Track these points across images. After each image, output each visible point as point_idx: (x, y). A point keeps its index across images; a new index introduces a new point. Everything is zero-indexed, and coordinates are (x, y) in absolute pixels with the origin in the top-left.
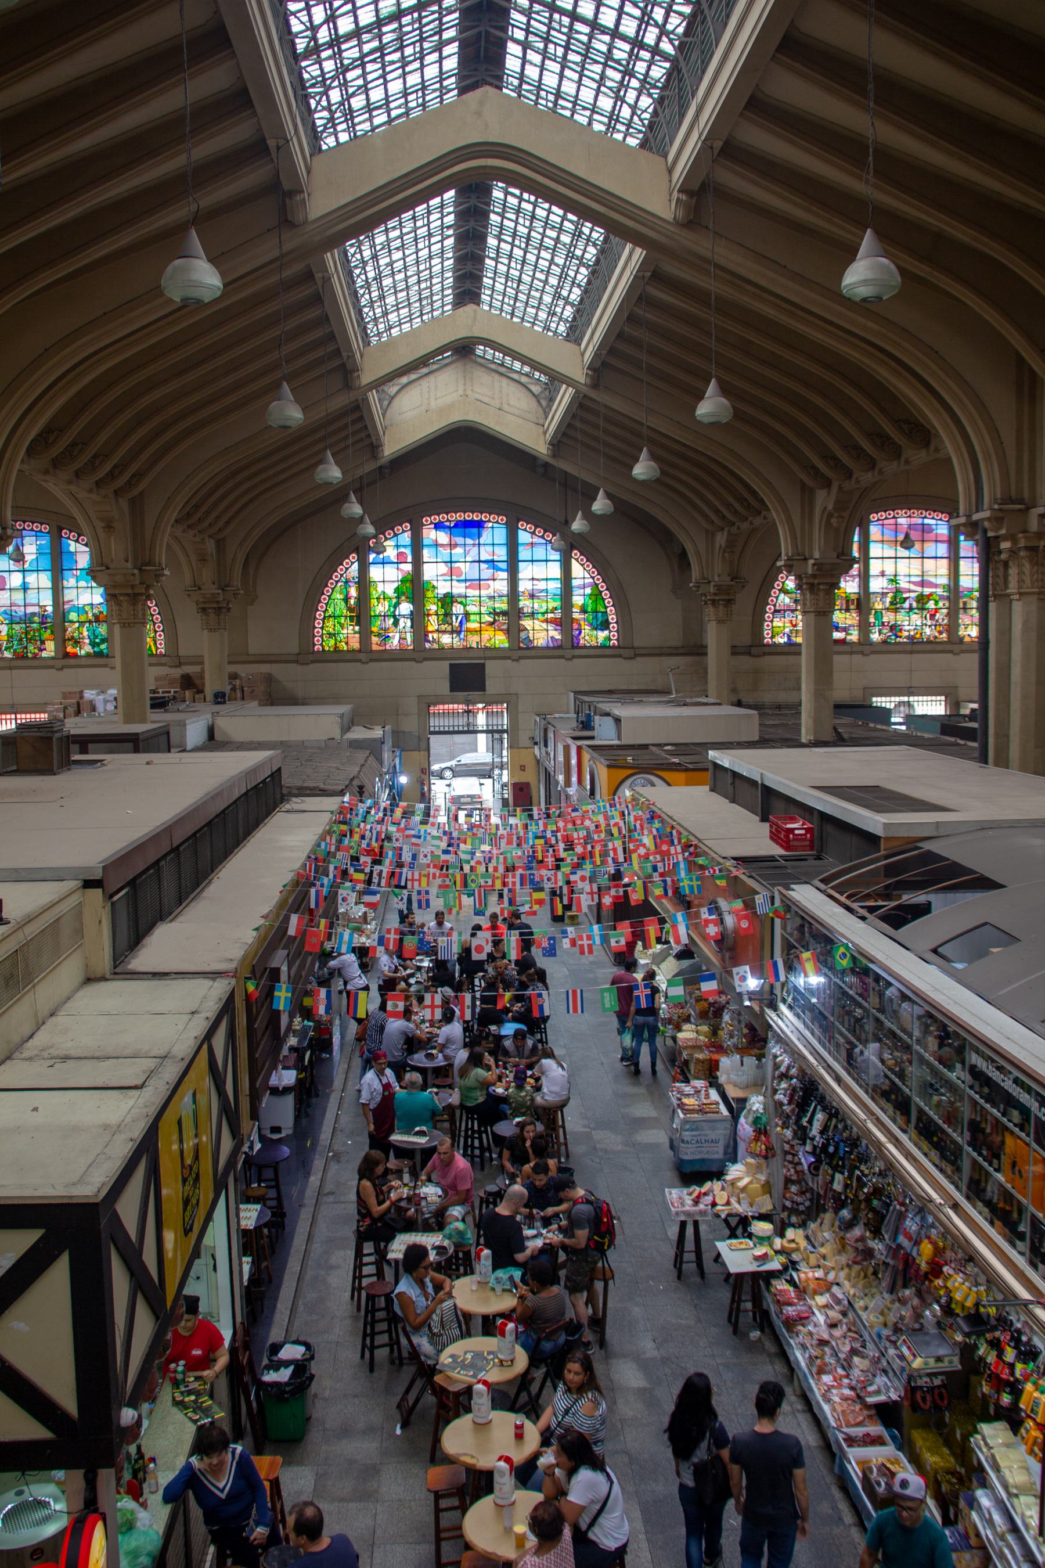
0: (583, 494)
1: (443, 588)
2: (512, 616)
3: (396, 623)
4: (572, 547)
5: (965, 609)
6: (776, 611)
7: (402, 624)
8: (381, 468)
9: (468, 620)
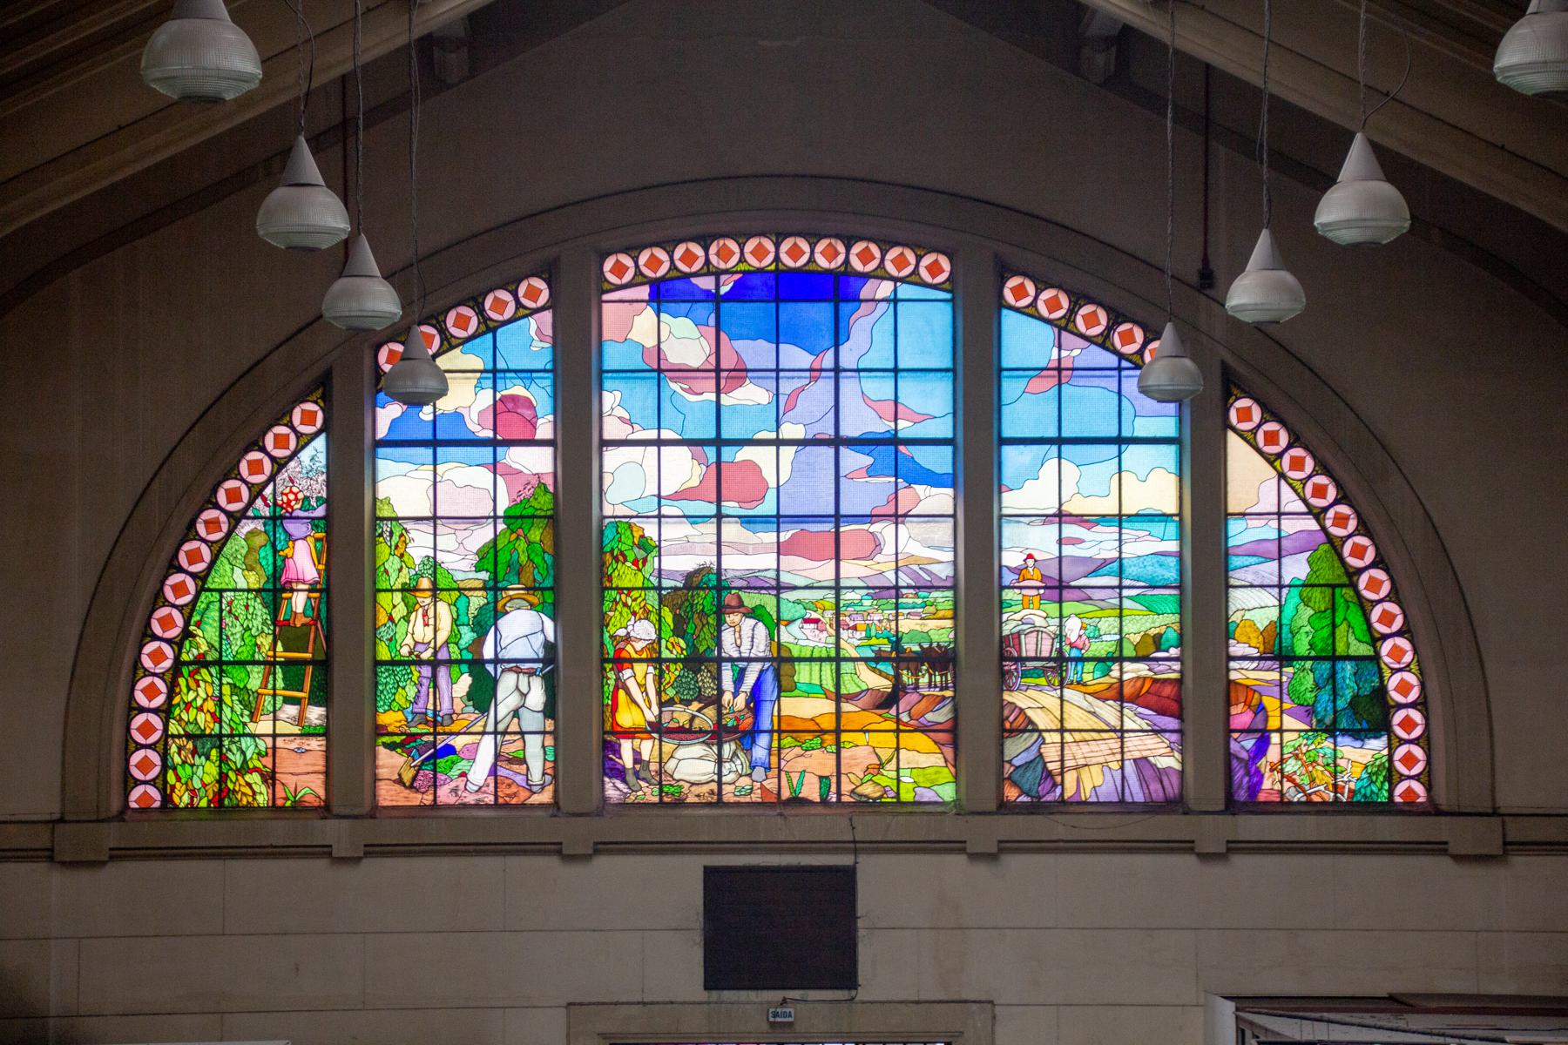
0: (1281, 162)
1: (683, 551)
2: (969, 669)
3: (483, 694)
4: (1231, 385)
7: (506, 698)
8: (428, 43)
9: (785, 686)
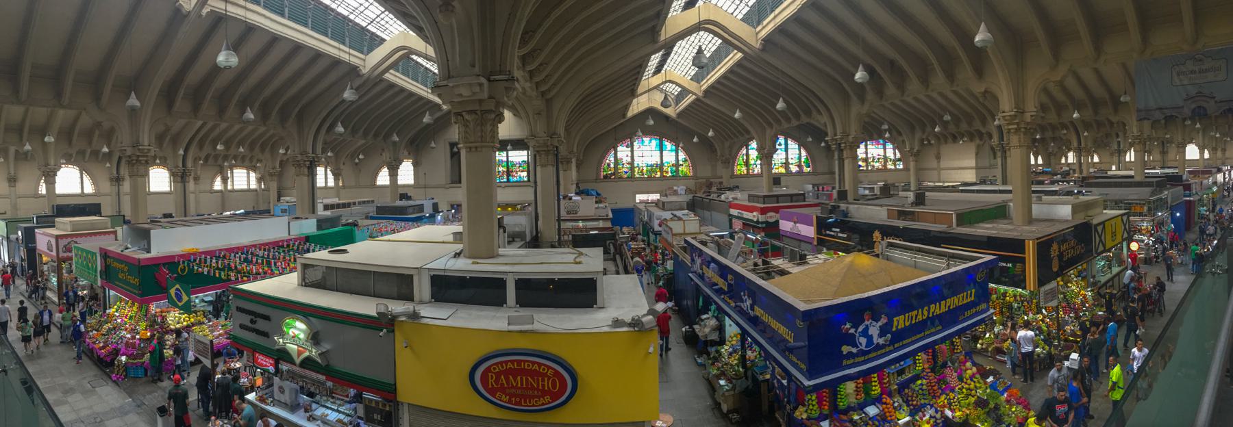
2: (786, 164)
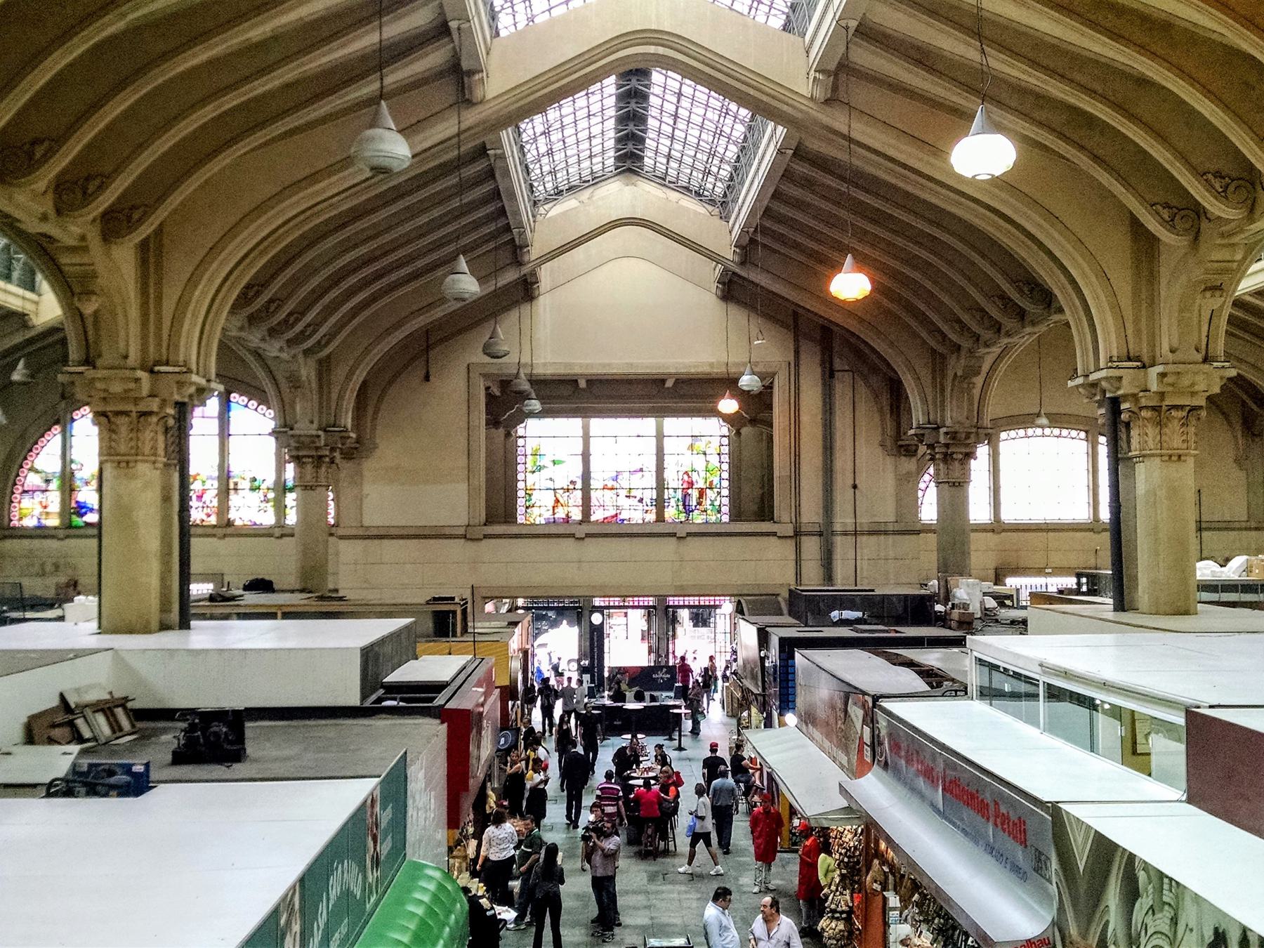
5: (236, 489)
6: (25, 492)
